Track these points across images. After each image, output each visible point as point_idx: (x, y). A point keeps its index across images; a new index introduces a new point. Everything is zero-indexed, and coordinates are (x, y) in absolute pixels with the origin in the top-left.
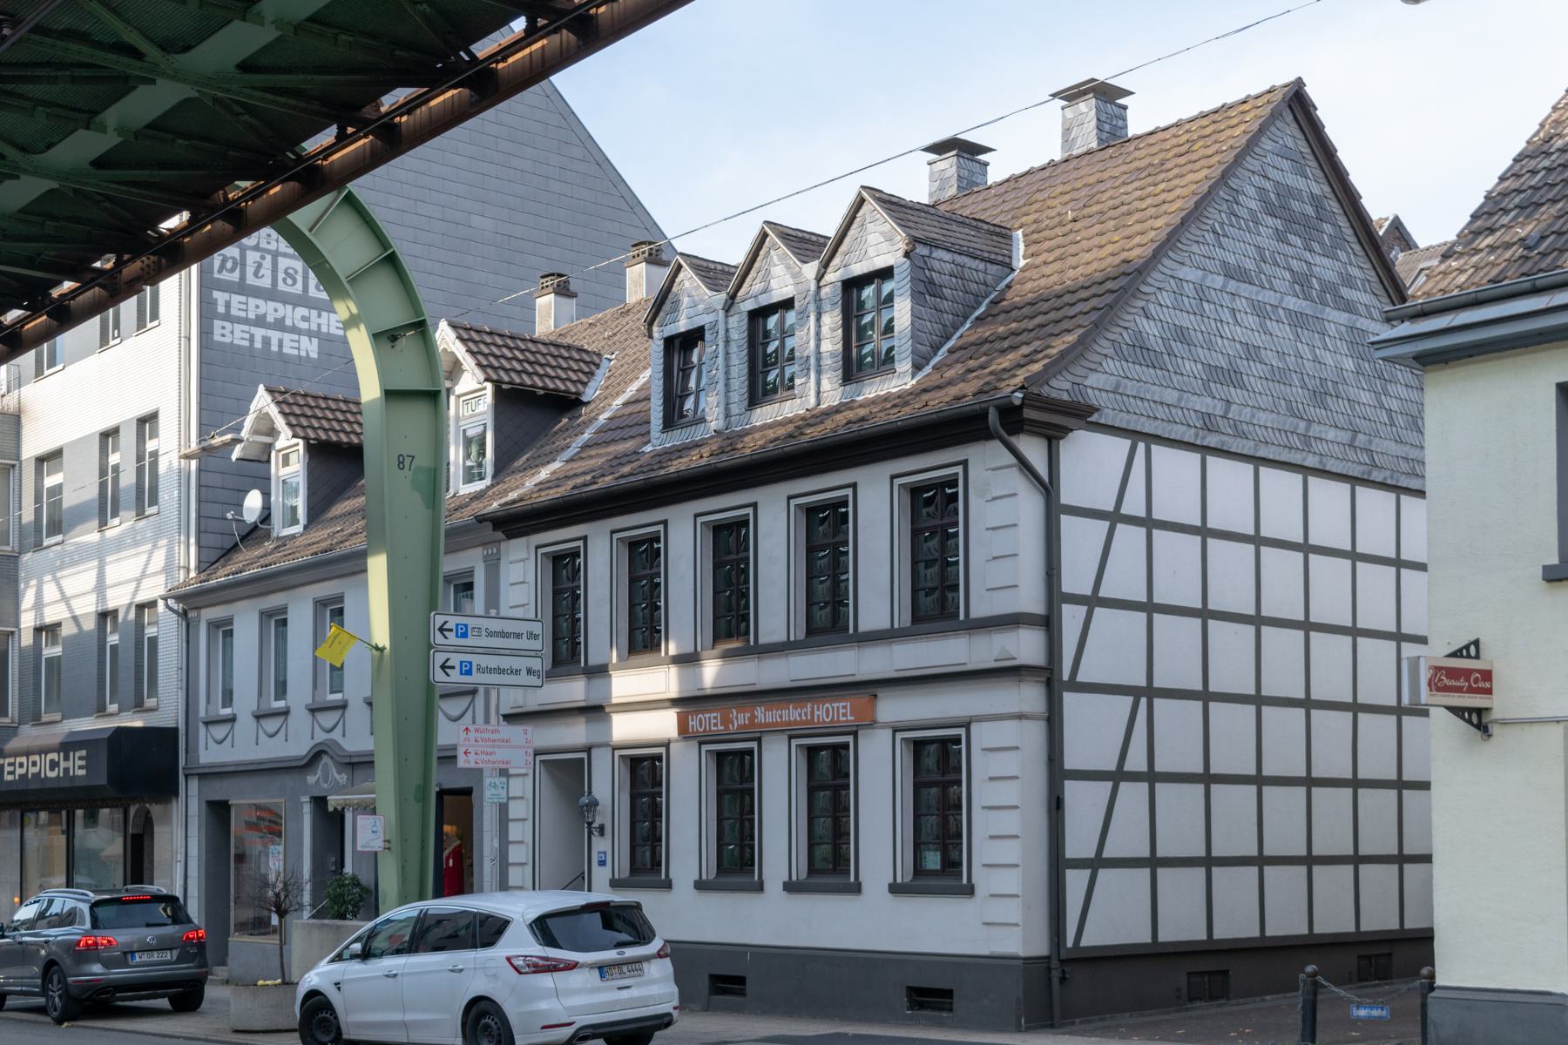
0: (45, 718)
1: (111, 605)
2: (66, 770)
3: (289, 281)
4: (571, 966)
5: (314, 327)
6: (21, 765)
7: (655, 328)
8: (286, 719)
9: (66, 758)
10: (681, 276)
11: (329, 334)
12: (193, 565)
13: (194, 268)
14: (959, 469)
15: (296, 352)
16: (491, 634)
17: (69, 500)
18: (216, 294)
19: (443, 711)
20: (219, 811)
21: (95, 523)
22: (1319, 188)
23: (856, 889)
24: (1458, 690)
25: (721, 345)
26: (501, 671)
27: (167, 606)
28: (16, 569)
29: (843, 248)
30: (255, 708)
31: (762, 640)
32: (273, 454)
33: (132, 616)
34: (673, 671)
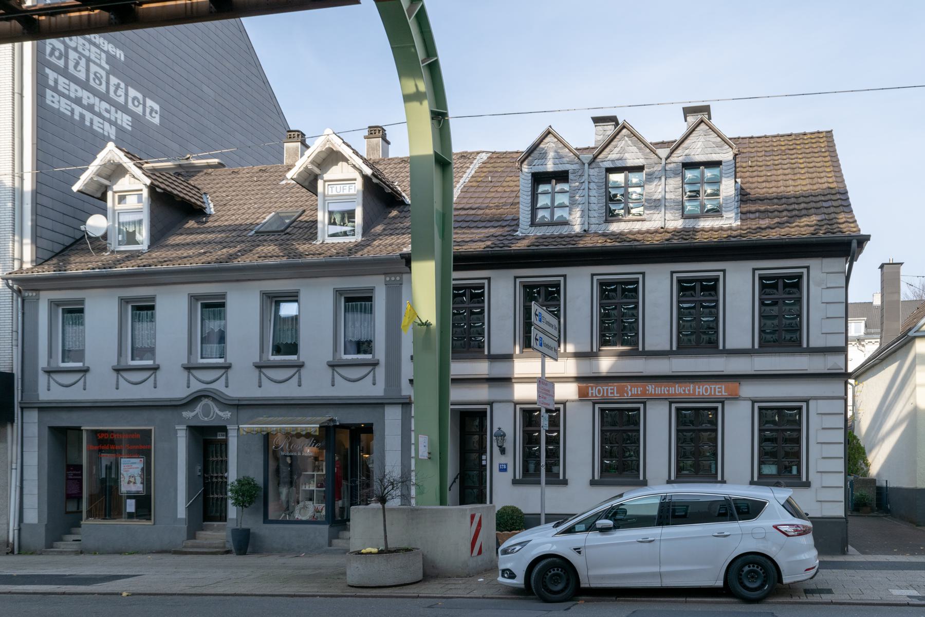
3: (97, 81)
5: (113, 119)
8: (373, 369)
11: (122, 126)
15: (101, 131)
19: (265, 375)
30: (331, 359)
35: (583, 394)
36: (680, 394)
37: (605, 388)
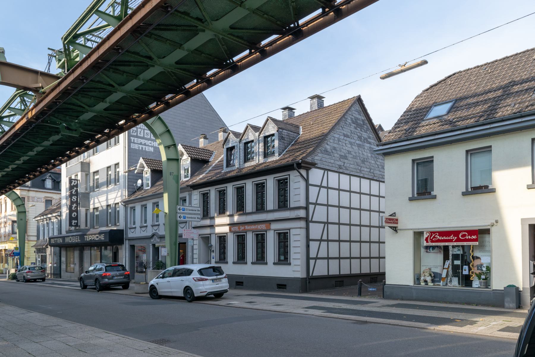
0: (95, 227)
1: (109, 203)
2: (100, 238)
3: (147, 135)
4: (206, 280)
5: (152, 145)
6: (90, 237)
7: (224, 146)
9: (100, 236)
10: (230, 135)
11: (156, 147)
12: (127, 195)
13: (127, 132)
14: (288, 176)
15: (148, 150)
16: (190, 210)
17: (100, 181)
18: (131, 138)
20: (132, 247)
21: (106, 186)
22: (364, 118)
23: (266, 264)
24: (391, 223)
25: (238, 150)
26: (192, 218)
27: (121, 204)
28: (89, 196)
29: (264, 130)
31: (247, 212)
32: (144, 172)
33: (114, 206)
34: (228, 218)
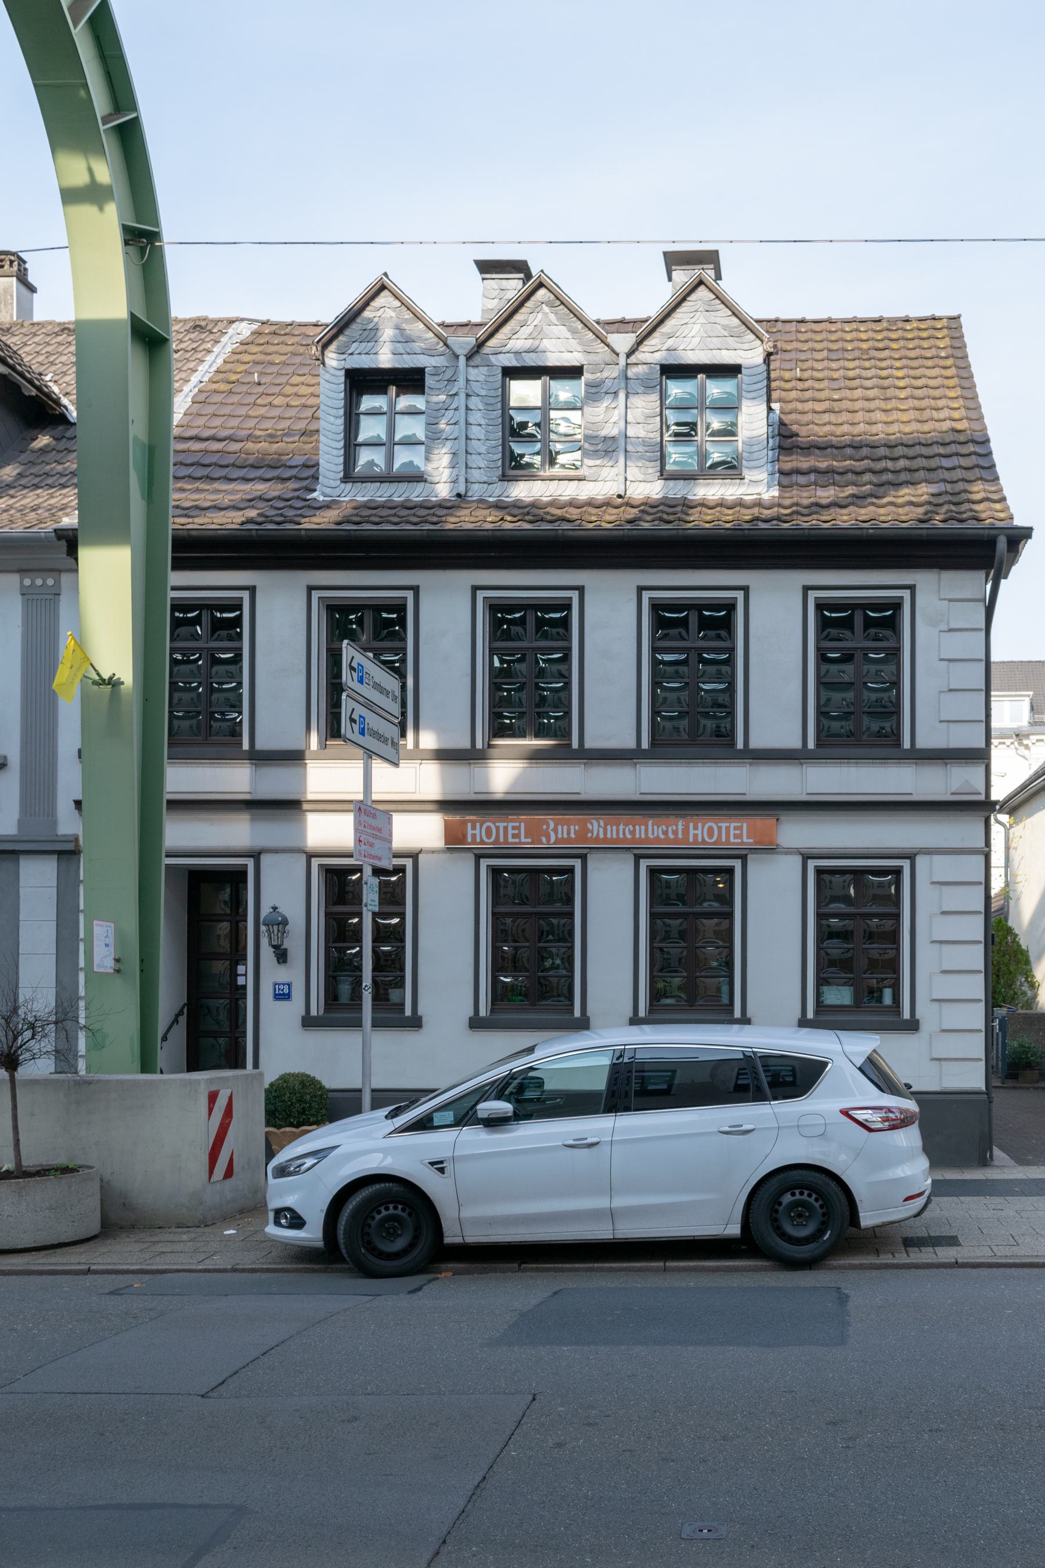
29: (665, 329)
31: (588, 744)
35: (454, 839)
36: (657, 839)
37: (502, 825)
